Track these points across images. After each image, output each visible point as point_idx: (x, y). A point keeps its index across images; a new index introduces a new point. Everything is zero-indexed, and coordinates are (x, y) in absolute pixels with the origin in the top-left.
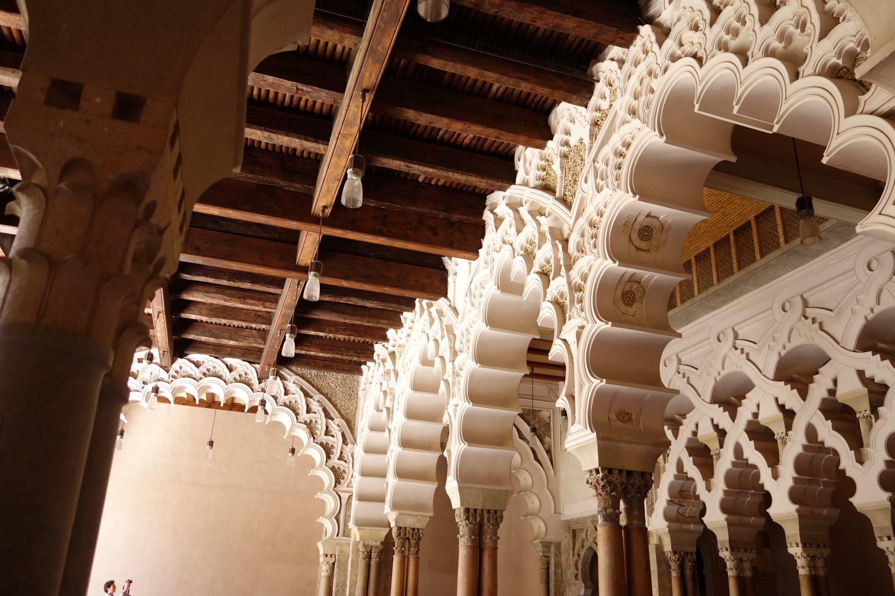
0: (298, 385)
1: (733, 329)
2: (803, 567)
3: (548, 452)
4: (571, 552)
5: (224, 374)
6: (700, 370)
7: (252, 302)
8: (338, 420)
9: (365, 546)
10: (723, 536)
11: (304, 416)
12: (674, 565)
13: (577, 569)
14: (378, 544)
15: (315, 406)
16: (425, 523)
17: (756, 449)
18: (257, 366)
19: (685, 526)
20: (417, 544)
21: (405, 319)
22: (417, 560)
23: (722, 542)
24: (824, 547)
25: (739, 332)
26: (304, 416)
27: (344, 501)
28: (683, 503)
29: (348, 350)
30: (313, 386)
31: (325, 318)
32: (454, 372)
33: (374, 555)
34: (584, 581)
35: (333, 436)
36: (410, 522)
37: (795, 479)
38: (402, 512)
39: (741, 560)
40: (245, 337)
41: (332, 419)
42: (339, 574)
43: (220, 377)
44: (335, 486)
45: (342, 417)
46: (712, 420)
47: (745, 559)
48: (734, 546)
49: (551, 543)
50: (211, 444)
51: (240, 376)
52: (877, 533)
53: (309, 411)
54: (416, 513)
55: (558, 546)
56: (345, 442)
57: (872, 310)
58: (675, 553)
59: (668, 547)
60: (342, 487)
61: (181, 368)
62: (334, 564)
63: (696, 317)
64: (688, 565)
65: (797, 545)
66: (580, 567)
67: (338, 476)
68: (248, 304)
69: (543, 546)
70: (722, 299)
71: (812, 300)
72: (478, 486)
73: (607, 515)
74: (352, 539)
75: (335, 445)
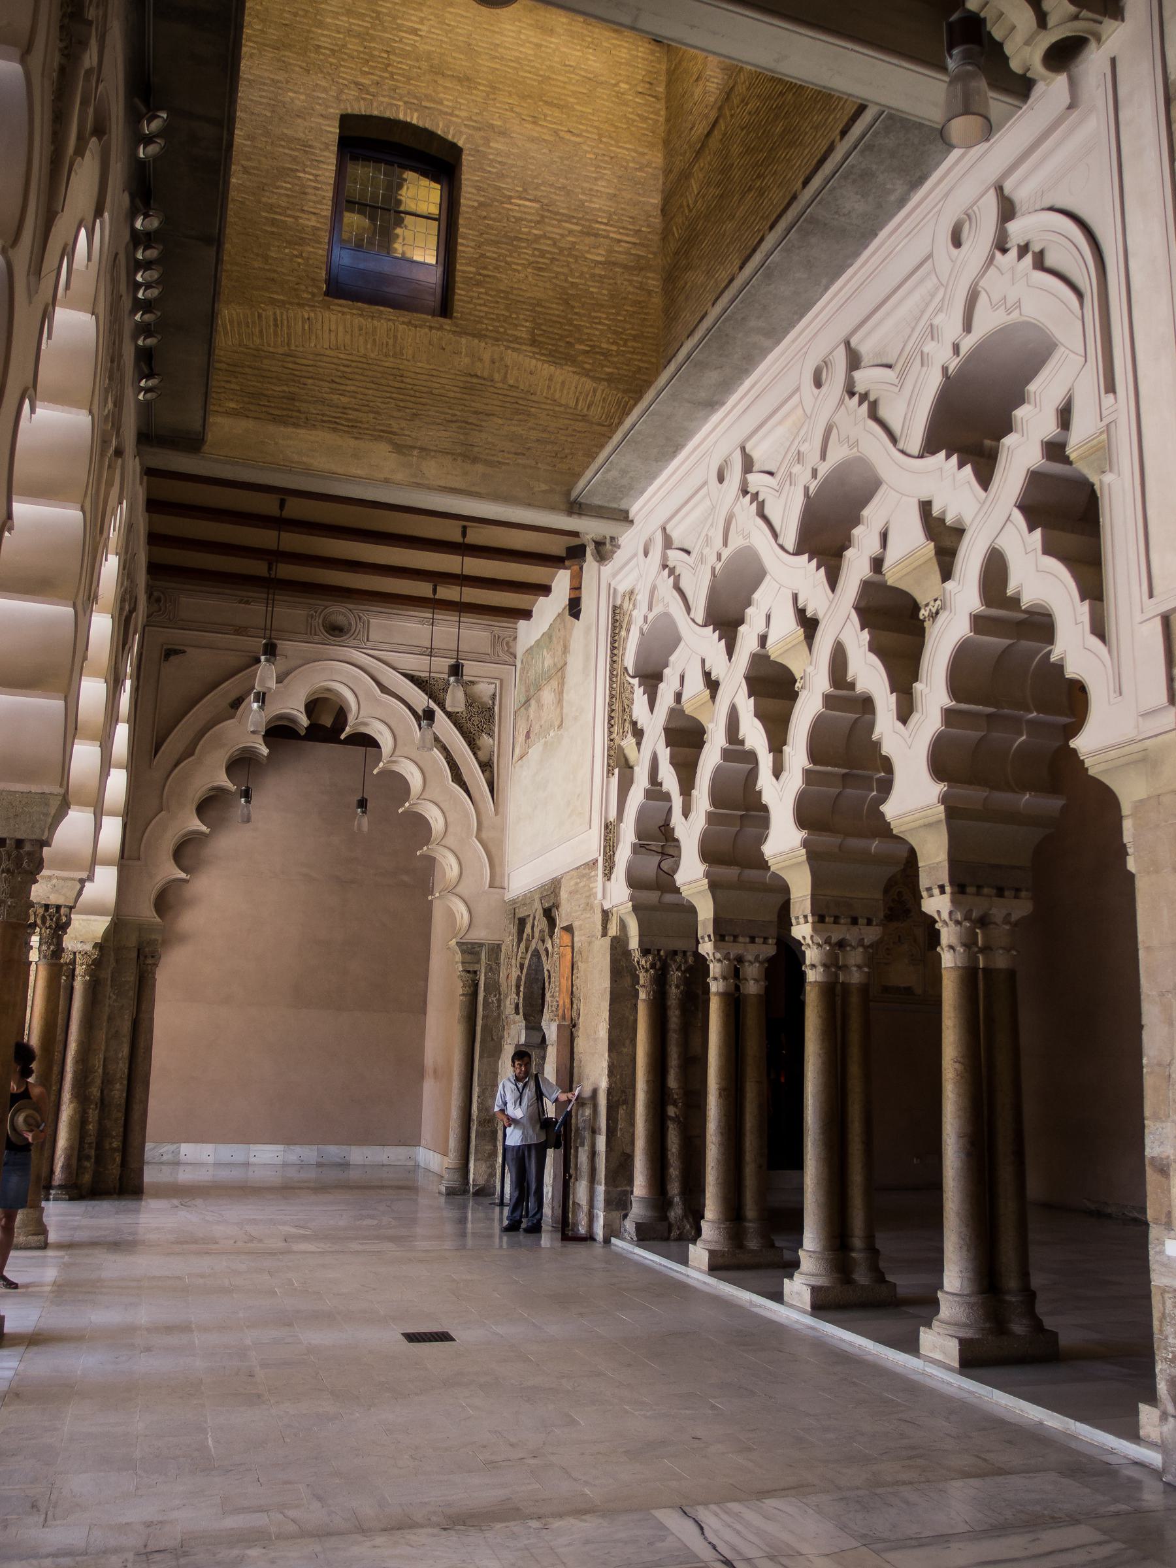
1: (743, 449)
3: (486, 766)
6: (694, 555)
12: (643, 978)
13: (518, 994)
14: (88, 947)
17: (756, 715)
24: (869, 922)
25: (756, 455)
46: (703, 661)
47: (750, 957)
49: (481, 945)
52: (924, 881)
55: (495, 950)
57: (956, 349)
58: (645, 952)
63: (689, 434)
64: (675, 976)
70: (713, 377)
71: (866, 348)
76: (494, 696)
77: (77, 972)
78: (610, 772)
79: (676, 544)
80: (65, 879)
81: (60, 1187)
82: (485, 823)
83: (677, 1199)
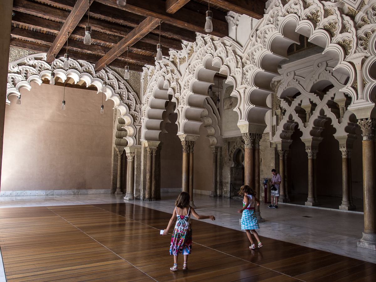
0: (114, 75)
2: (310, 156)
3: (218, 109)
4: (227, 150)
5: (78, 68)
7: (115, 31)
8: (133, 93)
9: (150, 149)
10: (308, 144)
11: (117, 90)
12: (281, 155)
14: (156, 148)
15: (122, 86)
16: (196, 139)
18: (94, 65)
19: (287, 141)
20: (193, 148)
21: (186, 46)
22: (193, 154)
23: (308, 146)
25: (329, 64)
26: (117, 90)
27: (138, 130)
28: (287, 132)
29: (144, 59)
30: (120, 76)
31: (148, 42)
32: (243, 73)
33: (154, 153)
34: (234, 161)
35: (131, 100)
36: (191, 138)
37: (349, 123)
38: (188, 134)
39: (314, 153)
40: (95, 49)
41: (130, 92)
42: (137, 160)
43: (77, 69)
44: (133, 123)
45: (134, 92)
47: (315, 153)
48: (313, 147)
50: (64, 102)
51: (86, 69)
53: (119, 88)
54: (194, 135)
55: (221, 148)
56: (136, 103)
59: (280, 148)
60: (137, 123)
61: (56, 64)
62: (134, 156)
64: (286, 155)
65: (344, 148)
66: (232, 156)
67: (134, 118)
68: (113, 31)
69: (215, 148)
72: (255, 124)
73: (370, 136)
74: (143, 146)
75: (132, 104)
76: (219, 95)
77: (153, 153)
78: (272, 116)
79: (296, 75)
80: (197, 136)
81: (153, 198)
82: (219, 122)
83: (287, 195)
